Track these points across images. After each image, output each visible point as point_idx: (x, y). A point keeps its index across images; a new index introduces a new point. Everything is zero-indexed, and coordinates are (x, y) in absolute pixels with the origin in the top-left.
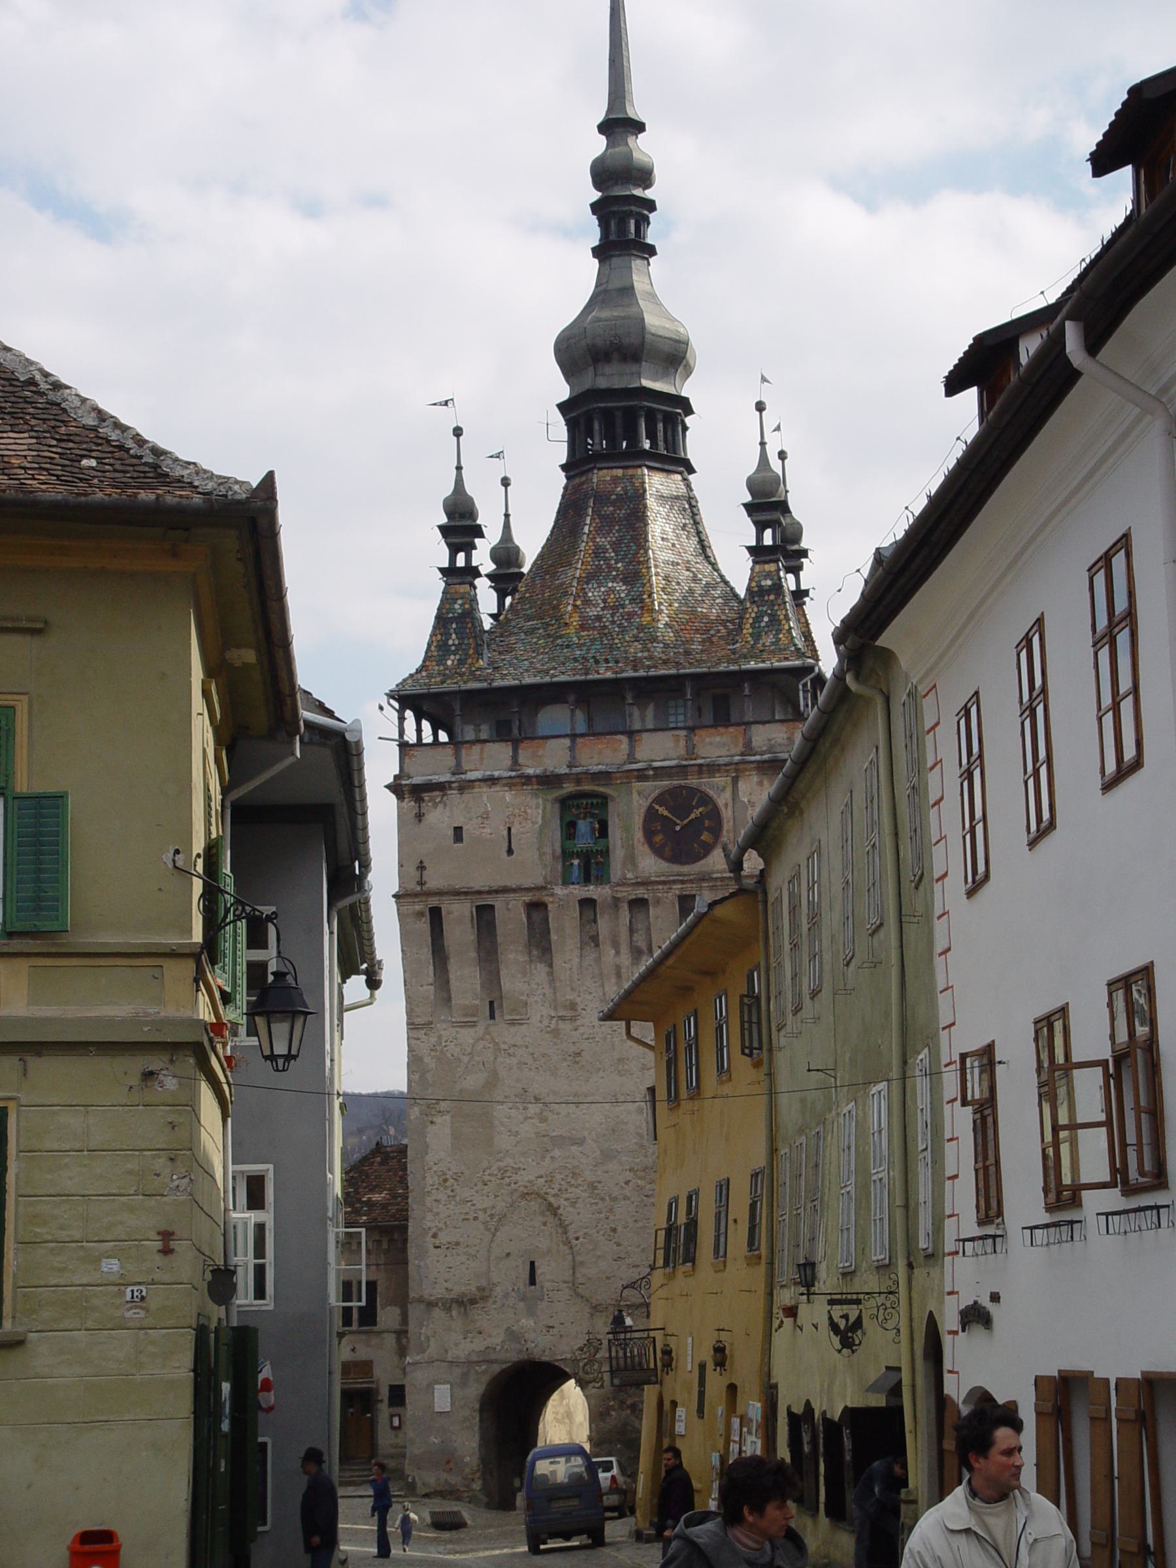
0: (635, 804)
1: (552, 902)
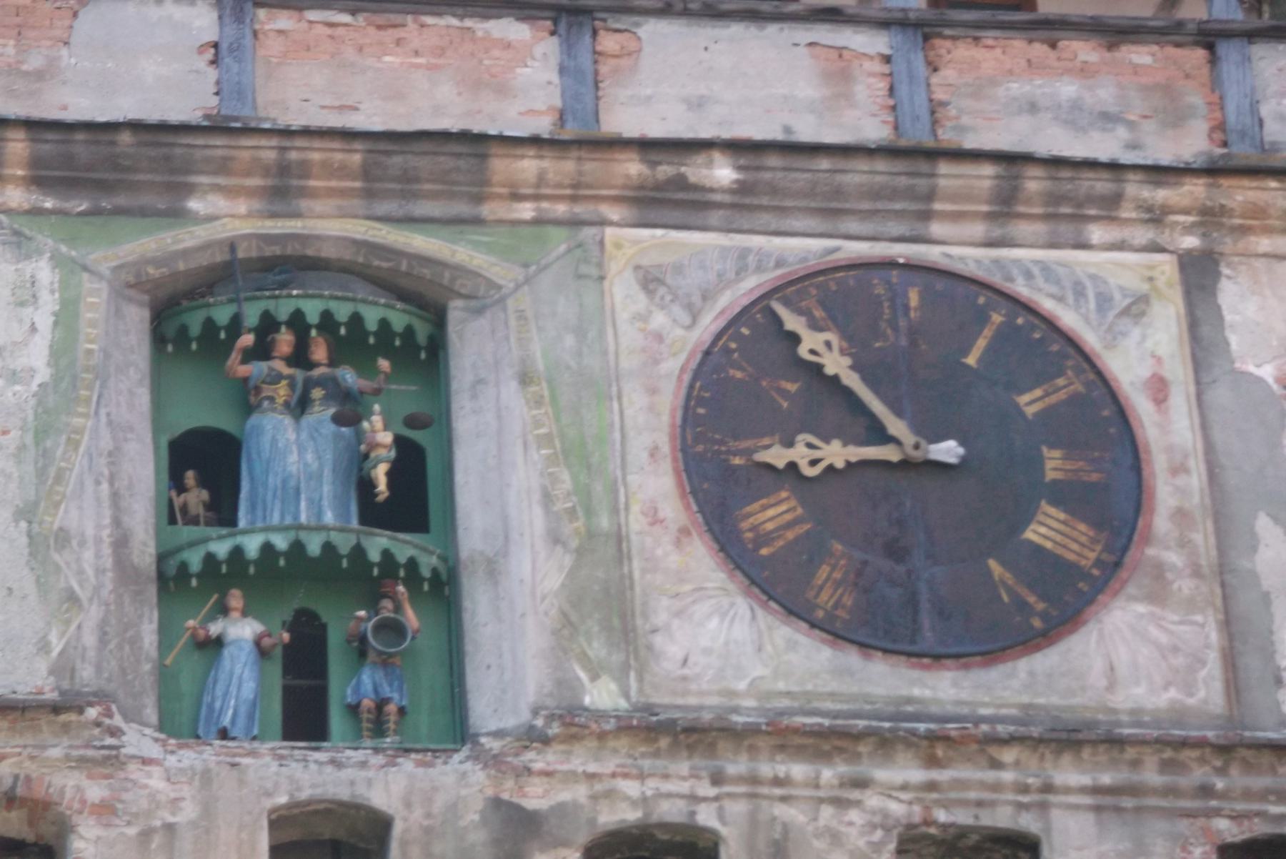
0: (629, 336)
1: (105, 810)
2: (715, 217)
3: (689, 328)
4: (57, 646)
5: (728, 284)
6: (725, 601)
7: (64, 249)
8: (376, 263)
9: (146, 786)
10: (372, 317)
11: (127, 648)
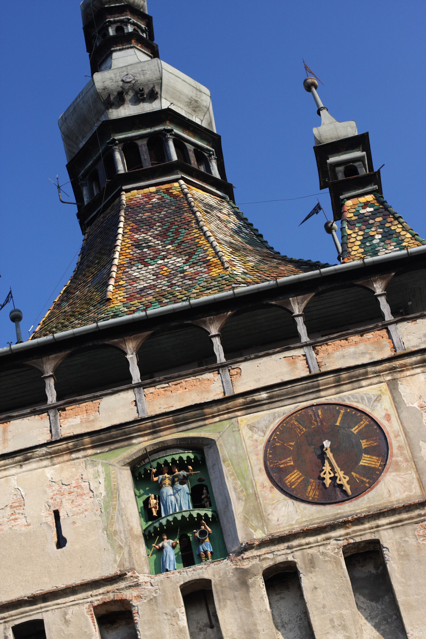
0: (249, 442)
1: (139, 597)
2: (265, 407)
3: (263, 436)
4: (118, 559)
5: (272, 422)
6: (286, 502)
7: (104, 461)
8: (183, 443)
9: (147, 589)
10: (184, 457)
11: (137, 555)
